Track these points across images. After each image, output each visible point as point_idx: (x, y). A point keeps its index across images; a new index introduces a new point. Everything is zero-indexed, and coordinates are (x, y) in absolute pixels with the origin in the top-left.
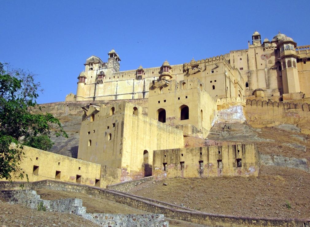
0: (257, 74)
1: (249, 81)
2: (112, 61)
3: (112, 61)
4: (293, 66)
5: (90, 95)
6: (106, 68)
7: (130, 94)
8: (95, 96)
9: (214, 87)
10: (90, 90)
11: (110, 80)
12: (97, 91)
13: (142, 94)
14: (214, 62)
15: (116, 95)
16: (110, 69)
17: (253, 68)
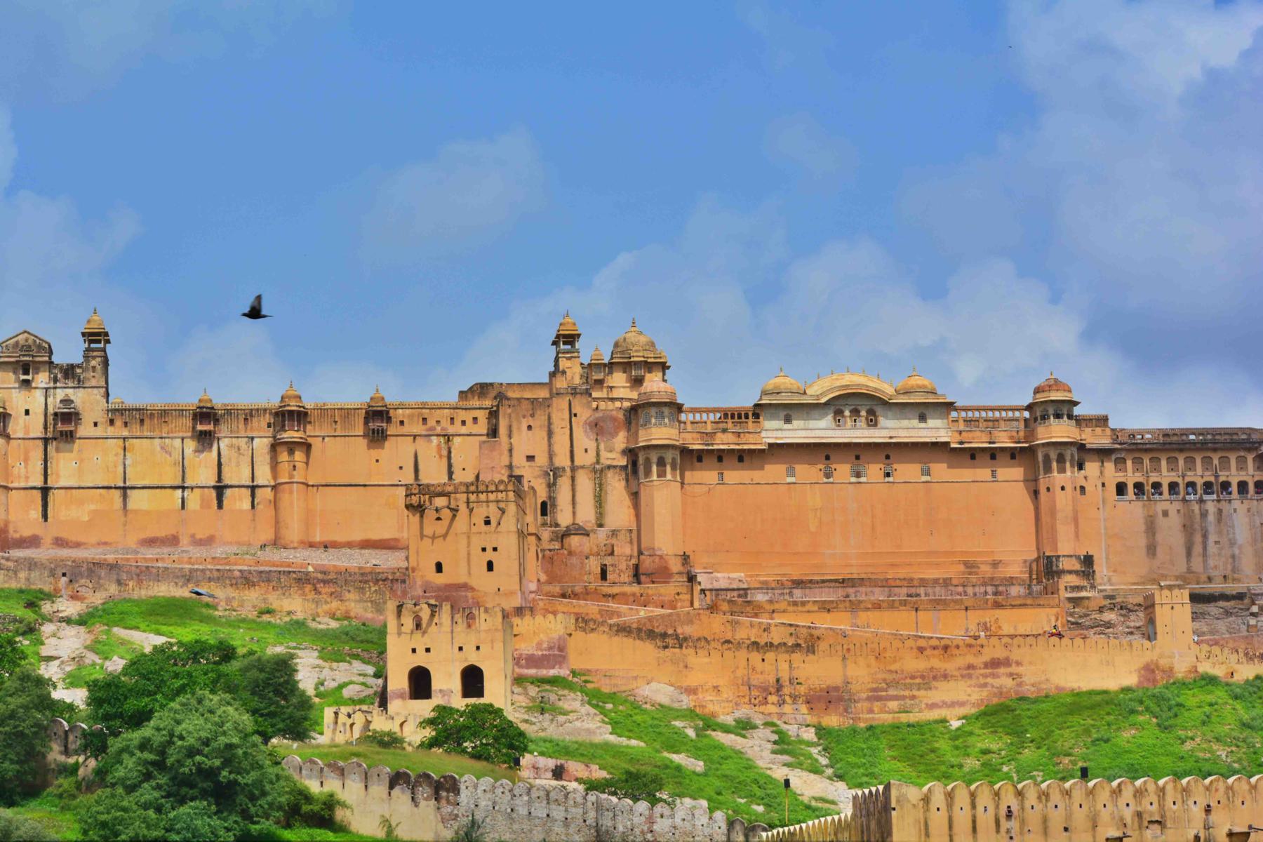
0: (573, 478)
1: (550, 497)
2: (99, 359)
3: (99, 359)
4: (669, 477)
5: (27, 478)
6: (80, 384)
7: (171, 487)
8: (46, 482)
9: (490, 566)
10: (26, 460)
11: (98, 432)
12: (54, 462)
13: (213, 493)
14: (492, 497)
15: (125, 489)
16: (95, 391)
17: (562, 460)
